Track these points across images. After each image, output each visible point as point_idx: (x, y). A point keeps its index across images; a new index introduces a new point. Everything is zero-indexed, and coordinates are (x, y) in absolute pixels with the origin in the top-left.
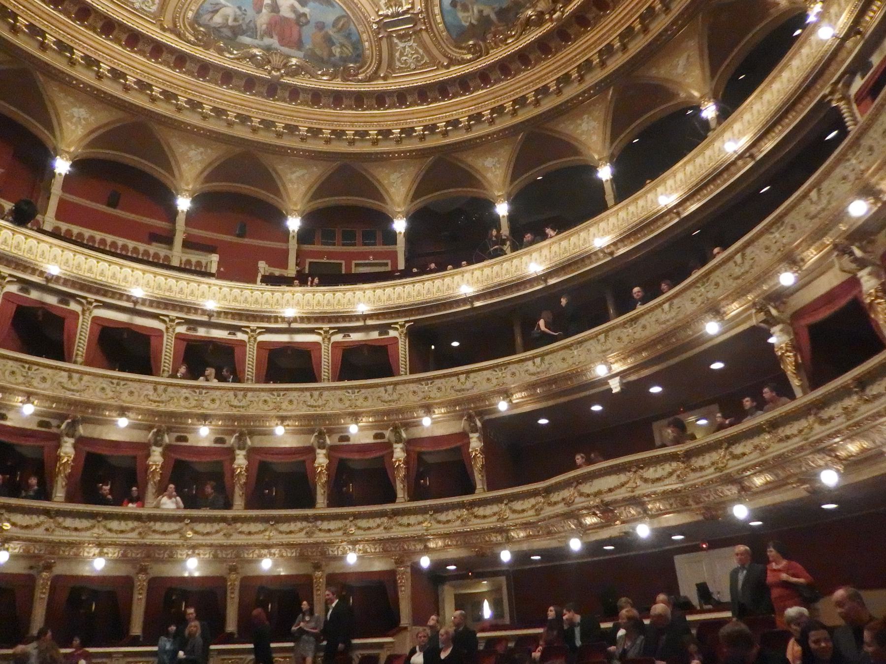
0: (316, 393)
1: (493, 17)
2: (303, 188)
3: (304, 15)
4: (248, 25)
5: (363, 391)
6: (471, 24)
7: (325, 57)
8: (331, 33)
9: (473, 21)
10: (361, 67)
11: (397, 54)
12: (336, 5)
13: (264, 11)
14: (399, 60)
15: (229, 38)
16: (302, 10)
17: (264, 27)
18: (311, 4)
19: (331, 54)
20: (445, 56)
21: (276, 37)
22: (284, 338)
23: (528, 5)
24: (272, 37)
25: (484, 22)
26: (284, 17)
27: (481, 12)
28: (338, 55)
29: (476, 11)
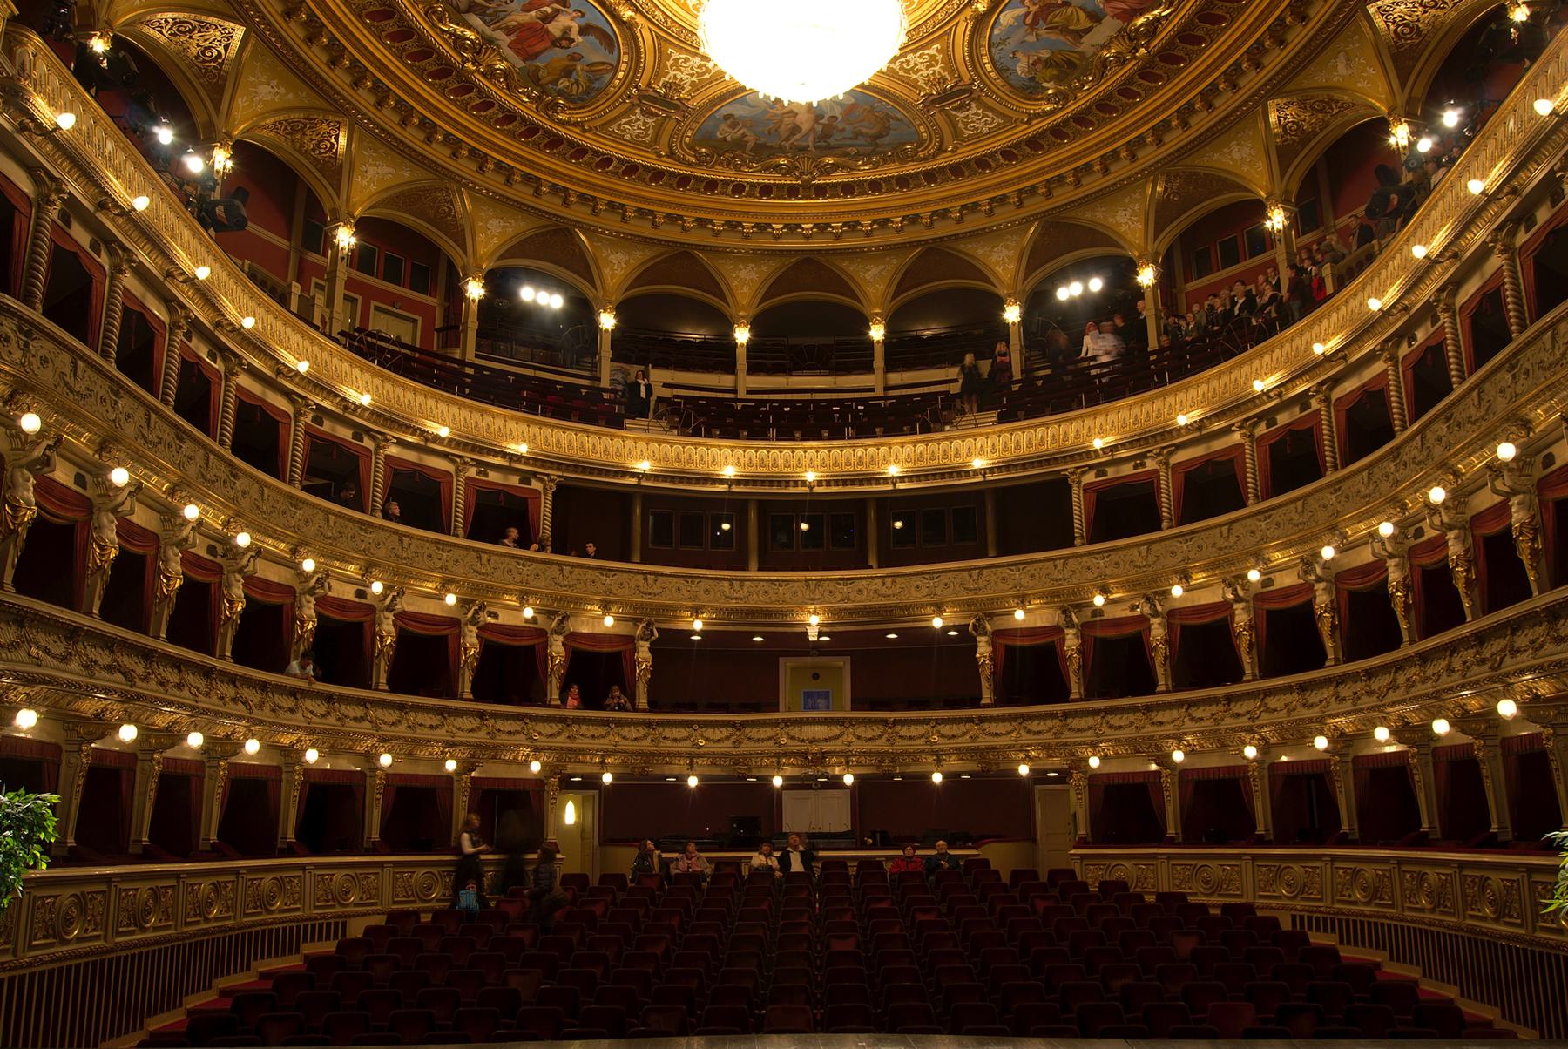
0: (484, 557)
1: (751, 145)
2: (373, 188)
3: (573, 41)
4: (496, 12)
5: (535, 565)
6: (725, 139)
7: (543, 82)
8: (579, 68)
9: (728, 139)
10: (570, 109)
11: (624, 121)
12: (616, 52)
13: (533, 13)
14: (619, 126)
15: (457, 9)
16: (574, 34)
17: (514, 23)
18: (591, 38)
19: (555, 82)
20: (670, 147)
21: (513, 37)
22: (411, 456)
23: (789, 155)
24: (508, 34)
25: (740, 144)
26: (547, 29)
27: (744, 135)
28: (560, 86)
29: (741, 132)
